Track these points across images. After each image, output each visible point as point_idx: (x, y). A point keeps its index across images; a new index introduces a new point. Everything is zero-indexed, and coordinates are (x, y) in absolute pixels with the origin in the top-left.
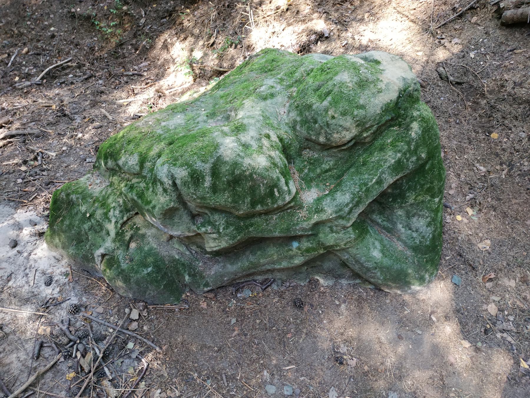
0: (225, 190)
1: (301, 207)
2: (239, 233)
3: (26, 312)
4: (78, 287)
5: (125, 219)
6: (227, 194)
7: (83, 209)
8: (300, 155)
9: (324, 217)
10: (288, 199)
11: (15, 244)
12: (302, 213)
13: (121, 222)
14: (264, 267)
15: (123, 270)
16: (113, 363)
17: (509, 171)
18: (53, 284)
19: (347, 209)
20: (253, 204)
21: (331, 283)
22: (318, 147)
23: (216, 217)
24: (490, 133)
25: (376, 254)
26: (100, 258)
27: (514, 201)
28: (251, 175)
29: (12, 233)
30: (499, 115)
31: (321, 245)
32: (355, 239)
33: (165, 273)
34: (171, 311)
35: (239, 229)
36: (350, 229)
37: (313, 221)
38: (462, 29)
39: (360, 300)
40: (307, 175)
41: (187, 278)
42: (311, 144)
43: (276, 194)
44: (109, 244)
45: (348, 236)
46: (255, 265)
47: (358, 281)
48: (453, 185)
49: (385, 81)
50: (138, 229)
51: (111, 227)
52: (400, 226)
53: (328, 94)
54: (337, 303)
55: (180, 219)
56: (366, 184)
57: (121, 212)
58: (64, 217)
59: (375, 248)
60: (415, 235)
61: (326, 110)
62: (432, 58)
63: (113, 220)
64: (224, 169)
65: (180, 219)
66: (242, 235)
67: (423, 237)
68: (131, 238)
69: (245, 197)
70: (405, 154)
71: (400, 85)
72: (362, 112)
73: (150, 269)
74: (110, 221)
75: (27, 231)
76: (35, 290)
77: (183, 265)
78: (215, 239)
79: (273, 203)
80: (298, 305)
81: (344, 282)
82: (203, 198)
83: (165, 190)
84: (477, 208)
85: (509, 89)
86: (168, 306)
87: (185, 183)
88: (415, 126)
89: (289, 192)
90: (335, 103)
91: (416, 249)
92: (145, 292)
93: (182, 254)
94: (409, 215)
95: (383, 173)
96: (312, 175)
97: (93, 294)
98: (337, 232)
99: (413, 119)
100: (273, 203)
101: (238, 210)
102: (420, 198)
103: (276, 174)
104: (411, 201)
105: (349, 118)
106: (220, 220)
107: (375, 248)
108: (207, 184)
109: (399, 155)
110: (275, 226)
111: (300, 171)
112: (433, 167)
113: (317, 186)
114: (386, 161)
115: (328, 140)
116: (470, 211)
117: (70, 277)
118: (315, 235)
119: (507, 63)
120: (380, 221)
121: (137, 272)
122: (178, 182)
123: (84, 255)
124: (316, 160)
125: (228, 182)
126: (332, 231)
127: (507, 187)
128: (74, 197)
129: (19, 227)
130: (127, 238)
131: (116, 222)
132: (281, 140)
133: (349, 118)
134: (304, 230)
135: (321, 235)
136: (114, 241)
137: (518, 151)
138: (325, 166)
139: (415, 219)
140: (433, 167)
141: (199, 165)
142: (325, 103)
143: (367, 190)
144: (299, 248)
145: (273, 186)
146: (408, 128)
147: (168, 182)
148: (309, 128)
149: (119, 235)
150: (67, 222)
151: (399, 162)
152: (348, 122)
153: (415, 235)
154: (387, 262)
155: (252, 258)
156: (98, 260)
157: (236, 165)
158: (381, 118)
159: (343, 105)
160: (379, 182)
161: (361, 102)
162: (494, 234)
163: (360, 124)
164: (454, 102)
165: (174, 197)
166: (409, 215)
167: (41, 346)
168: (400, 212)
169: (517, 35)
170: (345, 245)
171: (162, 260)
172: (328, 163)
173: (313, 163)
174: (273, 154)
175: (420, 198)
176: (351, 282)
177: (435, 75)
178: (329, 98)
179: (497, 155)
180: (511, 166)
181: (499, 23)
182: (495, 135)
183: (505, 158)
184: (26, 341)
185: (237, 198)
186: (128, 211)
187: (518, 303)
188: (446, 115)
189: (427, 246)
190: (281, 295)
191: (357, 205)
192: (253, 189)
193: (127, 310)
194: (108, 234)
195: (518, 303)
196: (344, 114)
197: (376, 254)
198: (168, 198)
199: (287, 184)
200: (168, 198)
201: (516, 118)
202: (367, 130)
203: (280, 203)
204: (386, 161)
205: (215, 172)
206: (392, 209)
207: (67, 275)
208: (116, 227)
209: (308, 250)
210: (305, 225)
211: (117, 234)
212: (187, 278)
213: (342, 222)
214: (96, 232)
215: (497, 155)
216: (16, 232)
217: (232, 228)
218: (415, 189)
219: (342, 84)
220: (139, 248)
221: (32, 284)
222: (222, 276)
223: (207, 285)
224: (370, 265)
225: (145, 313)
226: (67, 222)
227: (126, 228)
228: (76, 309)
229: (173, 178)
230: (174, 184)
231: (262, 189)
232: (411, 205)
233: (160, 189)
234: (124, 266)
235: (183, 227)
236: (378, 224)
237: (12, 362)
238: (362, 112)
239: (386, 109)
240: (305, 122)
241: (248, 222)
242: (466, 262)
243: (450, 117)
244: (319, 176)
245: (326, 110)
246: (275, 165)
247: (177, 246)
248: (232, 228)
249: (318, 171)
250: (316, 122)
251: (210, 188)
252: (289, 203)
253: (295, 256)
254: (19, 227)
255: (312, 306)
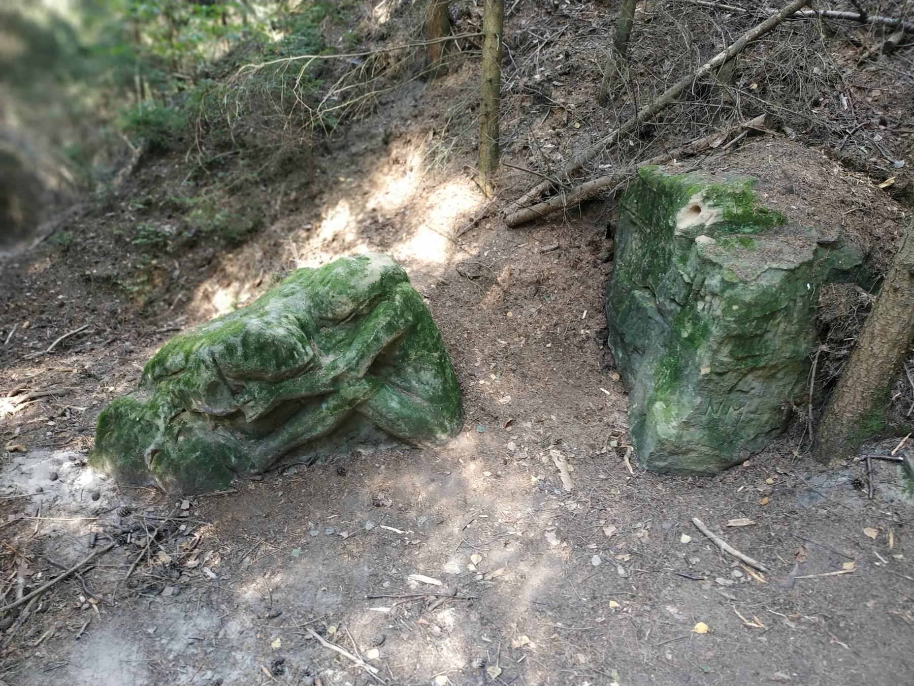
0: (253, 356)
1: (320, 368)
2: (271, 396)
3: (76, 520)
4: (126, 498)
5: (173, 414)
6: (256, 359)
7: (132, 416)
8: (318, 332)
9: (339, 372)
10: (306, 359)
11: (55, 477)
12: (322, 372)
13: (170, 417)
14: (303, 438)
15: (173, 460)
16: (167, 542)
17: (526, 341)
18: (101, 499)
19: (354, 362)
20: (278, 366)
21: (371, 451)
22: (330, 323)
23: (251, 384)
24: (506, 313)
25: (394, 404)
26: (150, 458)
27: (533, 364)
28: (273, 341)
29: (53, 468)
30: (512, 298)
31: (344, 400)
32: (371, 390)
33: (213, 458)
34: (221, 496)
35: (271, 392)
36: (363, 381)
37: (331, 377)
38: (478, 235)
39: (398, 460)
40: (325, 345)
41: (233, 459)
42: (325, 322)
43: (296, 356)
44: (159, 438)
45: (363, 387)
46: (294, 437)
47: (395, 445)
48: (479, 359)
49: (370, 270)
50: (185, 423)
51: (161, 423)
52: (414, 383)
53: (328, 282)
54: (377, 465)
55: (222, 395)
56: (366, 342)
57: (169, 408)
58: (113, 431)
59: (393, 399)
60: (427, 388)
61: (328, 293)
62: (453, 261)
63: (162, 416)
64: (251, 339)
65: (222, 395)
66: (274, 397)
67: (434, 388)
68: (180, 432)
69: (270, 360)
70: (393, 317)
71: (382, 271)
72: (353, 291)
73: (198, 454)
74: (159, 417)
75: (67, 465)
76: (84, 505)
77: (229, 448)
78: (252, 407)
79: (294, 363)
80: (341, 473)
81: (383, 448)
82: (237, 366)
83: (207, 367)
84: (499, 374)
85: (516, 275)
86: (217, 492)
87: (222, 356)
88: (398, 297)
89: (307, 354)
90: (333, 287)
91: (431, 400)
92: (195, 480)
93: (228, 439)
94: (417, 371)
95: (378, 332)
96: (329, 345)
97: (142, 500)
98: (353, 386)
99: (396, 293)
100: (294, 363)
101: (267, 373)
102: (419, 353)
103: (293, 340)
104: (413, 357)
105: (344, 295)
106: (254, 387)
107: (393, 399)
108: (239, 353)
109: (388, 318)
110: (300, 386)
111: (319, 343)
112: (423, 328)
113: (334, 353)
114: (379, 324)
115: (334, 314)
116: (493, 377)
117: (118, 490)
118: (336, 392)
119: (513, 256)
120: (399, 382)
121: (186, 458)
122: (217, 356)
123: (133, 462)
124: (332, 334)
125: (256, 349)
126: (350, 385)
127: (526, 354)
128: (122, 409)
129: (59, 463)
130: (176, 431)
131: (165, 418)
132: (298, 319)
133: (344, 295)
134: (325, 385)
135: (342, 391)
136: (164, 435)
137: (531, 323)
138: (339, 338)
139: (422, 373)
140: (423, 328)
141: (232, 340)
142: (327, 288)
143: (368, 346)
144: (328, 409)
145: (292, 349)
146: (394, 300)
147: (209, 359)
148: (320, 309)
149: (168, 429)
150: (115, 435)
151: (389, 323)
152: (344, 298)
153: (427, 388)
154: (406, 412)
155: (291, 430)
156: (147, 459)
157: (260, 335)
158: (370, 294)
159: (339, 288)
160: (377, 339)
161: (352, 284)
162: (515, 391)
163: (354, 299)
164: (475, 293)
165: (215, 373)
166: (417, 371)
167: (96, 539)
168: (410, 370)
169: (521, 233)
170: (364, 396)
171: (209, 446)
172: (341, 335)
173: (329, 337)
174: (290, 327)
175: (419, 353)
176: (389, 447)
177: (456, 273)
178: (329, 285)
179: (515, 330)
180: (527, 337)
181: (505, 226)
182: (510, 314)
183: (521, 331)
184: (81, 537)
185: (264, 362)
186: (175, 407)
187: (533, 437)
188: (468, 305)
189: (439, 396)
190: (325, 469)
191: (362, 357)
192: (276, 353)
193: (177, 504)
194: (158, 429)
195: (533, 437)
196: (340, 293)
197: (394, 404)
198: (210, 373)
199: (304, 348)
200: (210, 373)
201: (526, 298)
202: (362, 303)
203: (300, 363)
204: (379, 324)
205: (245, 343)
206: (403, 368)
207: (114, 490)
208: (165, 422)
209: (336, 408)
210: (324, 381)
211: (166, 428)
212: (233, 459)
213: (353, 374)
214: (146, 433)
215: (515, 330)
216: (56, 467)
217: (265, 392)
218: (413, 347)
219: (337, 274)
220: (187, 440)
221: (79, 500)
222: (266, 454)
223: (253, 467)
224: (391, 416)
225: (195, 503)
226: (115, 435)
227: (174, 423)
228: (127, 512)
229: (212, 354)
230: (214, 360)
231: (283, 351)
232: (415, 360)
233: (203, 367)
234: (174, 455)
235: (225, 403)
236: (398, 386)
237: (69, 553)
238: (353, 291)
239: (373, 287)
240: (316, 305)
241: (278, 386)
242: (489, 414)
243: (473, 305)
244: (335, 345)
245: (328, 293)
246: (293, 334)
247: (222, 433)
248: (265, 392)
249: (334, 341)
250: (323, 303)
251: (242, 356)
252: (309, 363)
253: (326, 417)
254: (59, 463)
255: (354, 472)
